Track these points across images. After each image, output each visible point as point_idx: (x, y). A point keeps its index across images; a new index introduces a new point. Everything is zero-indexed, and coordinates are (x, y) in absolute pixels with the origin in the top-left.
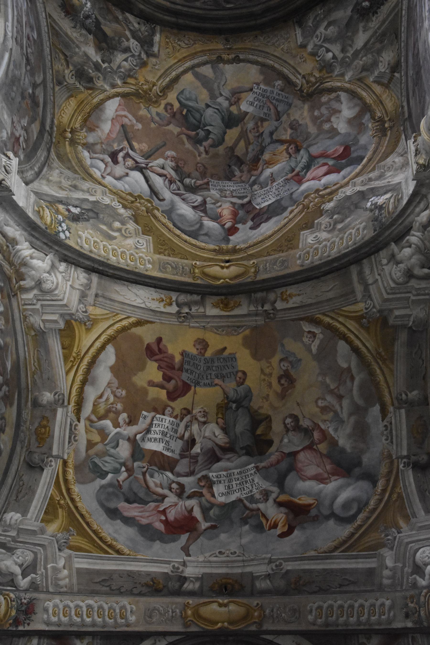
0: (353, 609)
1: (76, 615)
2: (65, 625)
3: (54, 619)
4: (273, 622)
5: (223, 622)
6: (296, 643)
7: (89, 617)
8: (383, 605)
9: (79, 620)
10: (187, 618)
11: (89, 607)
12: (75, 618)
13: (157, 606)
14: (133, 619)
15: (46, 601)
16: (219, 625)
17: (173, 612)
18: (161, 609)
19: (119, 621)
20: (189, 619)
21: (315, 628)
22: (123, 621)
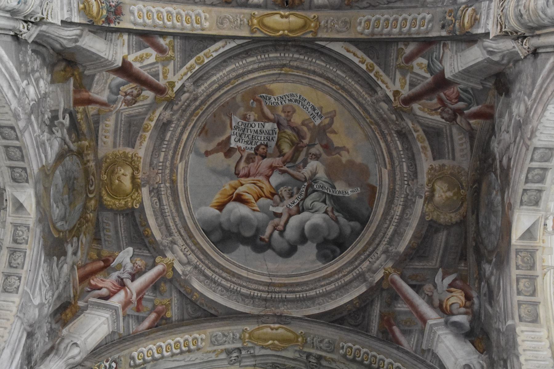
0: (397, 22)
1: (158, 19)
2: (150, 26)
3: (140, 21)
5: (284, 30)
6: (345, 48)
7: (169, 21)
8: (424, 18)
9: (161, 22)
10: (254, 25)
11: (169, 13)
12: (158, 21)
13: (227, 15)
14: (206, 24)
15: (131, 5)
16: (281, 32)
17: (241, 21)
18: (231, 17)
19: (195, 25)
20: (255, 27)
22: (199, 26)
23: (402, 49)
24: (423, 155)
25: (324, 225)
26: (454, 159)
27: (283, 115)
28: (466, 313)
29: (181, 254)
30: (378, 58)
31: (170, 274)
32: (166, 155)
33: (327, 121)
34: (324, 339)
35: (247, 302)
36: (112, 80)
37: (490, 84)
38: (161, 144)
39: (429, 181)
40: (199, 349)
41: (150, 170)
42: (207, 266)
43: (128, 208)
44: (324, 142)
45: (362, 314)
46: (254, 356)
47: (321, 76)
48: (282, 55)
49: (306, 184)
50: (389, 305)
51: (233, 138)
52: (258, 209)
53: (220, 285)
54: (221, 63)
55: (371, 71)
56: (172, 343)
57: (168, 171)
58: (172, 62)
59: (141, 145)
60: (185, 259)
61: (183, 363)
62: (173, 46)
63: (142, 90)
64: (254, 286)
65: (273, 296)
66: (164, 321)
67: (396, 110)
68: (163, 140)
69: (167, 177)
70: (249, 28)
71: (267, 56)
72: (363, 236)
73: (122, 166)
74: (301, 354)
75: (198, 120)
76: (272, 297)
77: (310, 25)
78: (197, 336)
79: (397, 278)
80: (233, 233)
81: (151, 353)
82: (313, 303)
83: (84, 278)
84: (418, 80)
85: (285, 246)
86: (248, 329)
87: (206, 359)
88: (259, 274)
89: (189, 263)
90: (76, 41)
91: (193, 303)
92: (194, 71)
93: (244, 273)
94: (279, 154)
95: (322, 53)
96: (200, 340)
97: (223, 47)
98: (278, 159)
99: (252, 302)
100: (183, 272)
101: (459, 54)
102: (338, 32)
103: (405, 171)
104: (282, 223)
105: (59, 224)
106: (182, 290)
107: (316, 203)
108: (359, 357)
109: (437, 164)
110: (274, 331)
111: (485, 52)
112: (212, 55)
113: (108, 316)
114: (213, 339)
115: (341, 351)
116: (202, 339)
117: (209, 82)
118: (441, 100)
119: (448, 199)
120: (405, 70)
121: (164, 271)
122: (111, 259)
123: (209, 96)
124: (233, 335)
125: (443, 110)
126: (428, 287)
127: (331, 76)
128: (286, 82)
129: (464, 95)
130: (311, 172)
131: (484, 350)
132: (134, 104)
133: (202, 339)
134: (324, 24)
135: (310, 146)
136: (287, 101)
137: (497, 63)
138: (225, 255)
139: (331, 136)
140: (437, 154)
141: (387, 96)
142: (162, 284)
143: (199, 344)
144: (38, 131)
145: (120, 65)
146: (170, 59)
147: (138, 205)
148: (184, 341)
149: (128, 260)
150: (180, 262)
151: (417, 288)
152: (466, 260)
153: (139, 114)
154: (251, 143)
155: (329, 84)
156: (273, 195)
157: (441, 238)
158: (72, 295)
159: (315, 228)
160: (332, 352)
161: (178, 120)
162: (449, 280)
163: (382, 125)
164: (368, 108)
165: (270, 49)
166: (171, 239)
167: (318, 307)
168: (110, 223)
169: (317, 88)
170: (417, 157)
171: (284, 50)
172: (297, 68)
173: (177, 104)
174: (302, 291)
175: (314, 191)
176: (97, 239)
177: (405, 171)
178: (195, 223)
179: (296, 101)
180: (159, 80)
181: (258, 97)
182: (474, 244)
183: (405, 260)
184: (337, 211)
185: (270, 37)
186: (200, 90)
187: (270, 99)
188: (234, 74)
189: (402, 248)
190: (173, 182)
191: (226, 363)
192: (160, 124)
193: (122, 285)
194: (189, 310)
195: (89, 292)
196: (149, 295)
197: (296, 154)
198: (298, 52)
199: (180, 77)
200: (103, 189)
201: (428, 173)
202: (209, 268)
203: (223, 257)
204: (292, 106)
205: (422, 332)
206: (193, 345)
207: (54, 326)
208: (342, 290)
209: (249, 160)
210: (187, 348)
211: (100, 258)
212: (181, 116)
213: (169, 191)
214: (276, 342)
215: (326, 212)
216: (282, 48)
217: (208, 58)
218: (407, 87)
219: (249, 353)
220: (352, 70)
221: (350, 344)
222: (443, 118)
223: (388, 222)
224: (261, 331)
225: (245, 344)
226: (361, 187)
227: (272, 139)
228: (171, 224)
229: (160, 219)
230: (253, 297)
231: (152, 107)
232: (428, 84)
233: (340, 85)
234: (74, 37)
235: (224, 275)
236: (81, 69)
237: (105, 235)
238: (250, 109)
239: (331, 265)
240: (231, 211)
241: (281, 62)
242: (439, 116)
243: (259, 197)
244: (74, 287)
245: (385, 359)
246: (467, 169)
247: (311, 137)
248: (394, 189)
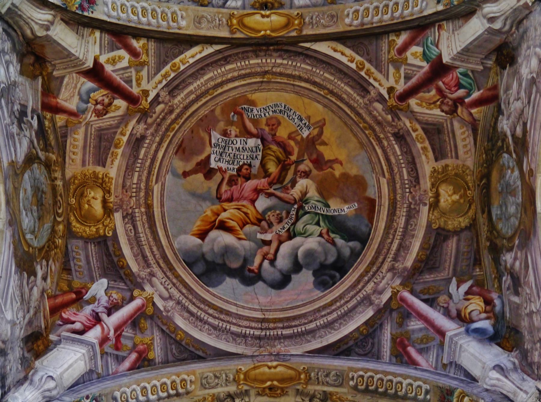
0: (388, 8)
1: (133, 14)
2: (124, 21)
3: (114, 14)
4: (312, 27)
5: (266, 31)
6: (331, 48)
7: (144, 17)
9: (135, 18)
10: (233, 25)
11: (143, 8)
12: (132, 16)
13: (205, 14)
14: (183, 23)
16: (263, 33)
17: (219, 21)
18: (209, 17)
19: (171, 23)
20: (235, 27)
21: (352, 28)
22: (175, 24)
23: (394, 41)
24: (423, 157)
25: (320, 249)
26: (457, 157)
27: (267, 129)
28: (487, 318)
29: (161, 288)
30: (368, 54)
31: (150, 310)
32: (139, 176)
33: (316, 132)
34: (330, 373)
35: (239, 341)
36: (81, 85)
37: (490, 63)
38: (134, 163)
39: (433, 185)
40: (188, 393)
41: (123, 192)
42: (191, 301)
43: (100, 236)
44: (314, 156)
45: (371, 340)
47: (307, 81)
48: (264, 61)
49: (296, 206)
50: (401, 325)
51: (213, 157)
52: (243, 237)
53: (206, 323)
54: (198, 70)
55: (362, 69)
56: (158, 384)
57: (142, 194)
58: (146, 68)
59: (112, 163)
60: (166, 294)
62: (147, 50)
63: (114, 99)
64: (246, 323)
65: (268, 334)
66: (146, 363)
67: (391, 109)
68: (136, 157)
69: (142, 201)
70: (228, 29)
71: (247, 63)
72: (365, 256)
73: (92, 188)
74: (304, 398)
75: (174, 136)
76: (266, 335)
77: (293, 23)
79: (407, 295)
80: (218, 264)
81: (135, 395)
82: (314, 337)
83: (55, 310)
84: (413, 71)
85: (277, 276)
86: (243, 369)
88: (250, 309)
89: (171, 297)
90: (48, 29)
91: (178, 343)
92: (169, 79)
93: (233, 309)
94: (263, 174)
95: (307, 56)
96: (189, 382)
97: (200, 53)
98: (263, 180)
99: (244, 341)
100: (165, 307)
101: (456, 33)
102: (325, 27)
103: (406, 177)
104: (272, 251)
105: (29, 236)
106: (164, 328)
107: (308, 226)
108: (372, 385)
109: (439, 165)
110: (273, 370)
111: (485, 21)
112: (188, 62)
113: (84, 351)
114: (204, 381)
115: (351, 383)
116: (191, 381)
117: (186, 92)
118: (440, 91)
119: (454, 202)
120: (397, 63)
121: (143, 305)
122: (84, 291)
123: (186, 108)
124: (227, 376)
125: (442, 102)
126: (442, 299)
127: (317, 80)
128: (269, 90)
129: (464, 81)
130: (301, 192)
131: (513, 348)
132: (105, 115)
133: (191, 381)
134: (309, 21)
135: (298, 162)
136: (271, 113)
137: (499, 31)
138: (210, 289)
139: (321, 148)
140: (439, 154)
141: (381, 95)
142: (142, 321)
143: (188, 386)
144: (8, 121)
145: (91, 66)
146: (143, 64)
147: (111, 233)
148: (172, 383)
149: (103, 292)
150: (161, 297)
151: (430, 302)
152: (480, 264)
153: (111, 127)
154: (233, 163)
155: (316, 90)
156: (260, 221)
157: (452, 245)
158: (43, 326)
159: (310, 254)
160: (341, 385)
161: (153, 135)
162: (465, 287)
163: (377, 128)
164: (361, 111)
165: (250, 54)
166: (149, 270)
167: (319, 340)
168: (81, 252)
169: (303, 95)
170: (417, 161)
171: (265, 55)
172: (281, 74)
173: (151, 117)
174: (300, 325)
175: (306, 213)
176: (66, 268)
177: (406, 177)
178: (175, 254)
179: (281, 111)
180: (131, 87)
181: (239, 109)
182: (488, 244)
183: (414, 274)
184: (333, 232)
185: (251, 38)
186: (176, 101)
187: (252, 110)
188: (212, 83)
189: (409, 263)
190: (149, 207)
192: (134, 139)
193: (97, 319)
194: (174, 351)
195: (60, 325)
196: (128, 332)
197: (283, 173)
198: (281, 57)
199: (154, 85)
200: (71, 214)
201: (431, 177)
202: (194, 304)
203: (208, 291)
204: (276, 118)
205: (441, 345)
207: (26, 355)
208: (346, 318)
209: (232, 181)
210: (175, 392)
211: (71, 290)
212: (156, 131)
213: (144, 217)
214: (275, 383)
215: (321, 235)
216: (262, 54)
217: (183, 64)
218: (402, 80)
220: (341, 71)
221: (361, 373)
222: (442, 111)
223: (391, 237)
224: (257, 371)
226: (359, 202)
227: (256, 157)
228: (148, 254)
229: (136, 248)
230: (245, 336)
231: (124, 119)
232: (425, 73)
233: (328, 89)
234: (46, 23)
235: (211, 311)
236: (50, 69)
237: (75, 265)
238: (232, 123)
239: (331, 292)
240: (214, 240)
241: (263, 69)
242: (439, 110)
243: (243, 225)
244: (44, 318)
245: (403, 381)
246: (472, 168)
247: (299, 153)
248: (395, 198)
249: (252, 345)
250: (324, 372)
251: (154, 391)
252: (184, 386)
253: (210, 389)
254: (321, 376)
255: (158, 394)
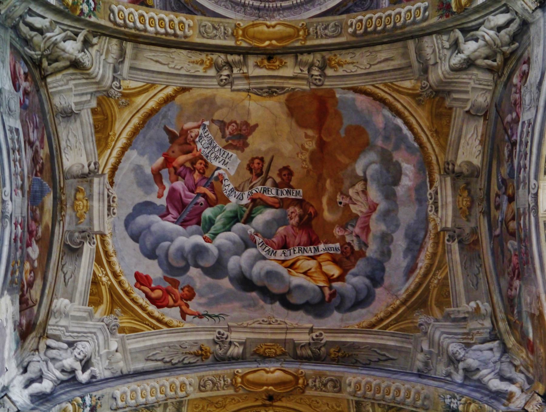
34: (328, 25)
35: (238, 9)
46: (247, 77)
56: (156, 17)
61: (165, 69)
65: (267, 5)
74: (302, 68)
76: (265, 6)
78: (184, 20)
81: (133, 18)
86: (242, 25)
87: (192, 72)
96: (187, 26)
99: (243, 10)
110: (271, 29)
114: (202, 29)
116: (189, 25)
124: (225, 29)
133: (189, 25)
160: (340, 35)
167: (318, 7)
191: (215, 82)
206: (180, 30)
214: (274, 42)
219: (241, 72)
224: (256, 29)
225: (238, 43)
249: (251, 15)
250: (323, 25)
251: (152, 24)
252: (182, 29)
253: (208, 38)
254: (320, 30)
255: (155, 27)
